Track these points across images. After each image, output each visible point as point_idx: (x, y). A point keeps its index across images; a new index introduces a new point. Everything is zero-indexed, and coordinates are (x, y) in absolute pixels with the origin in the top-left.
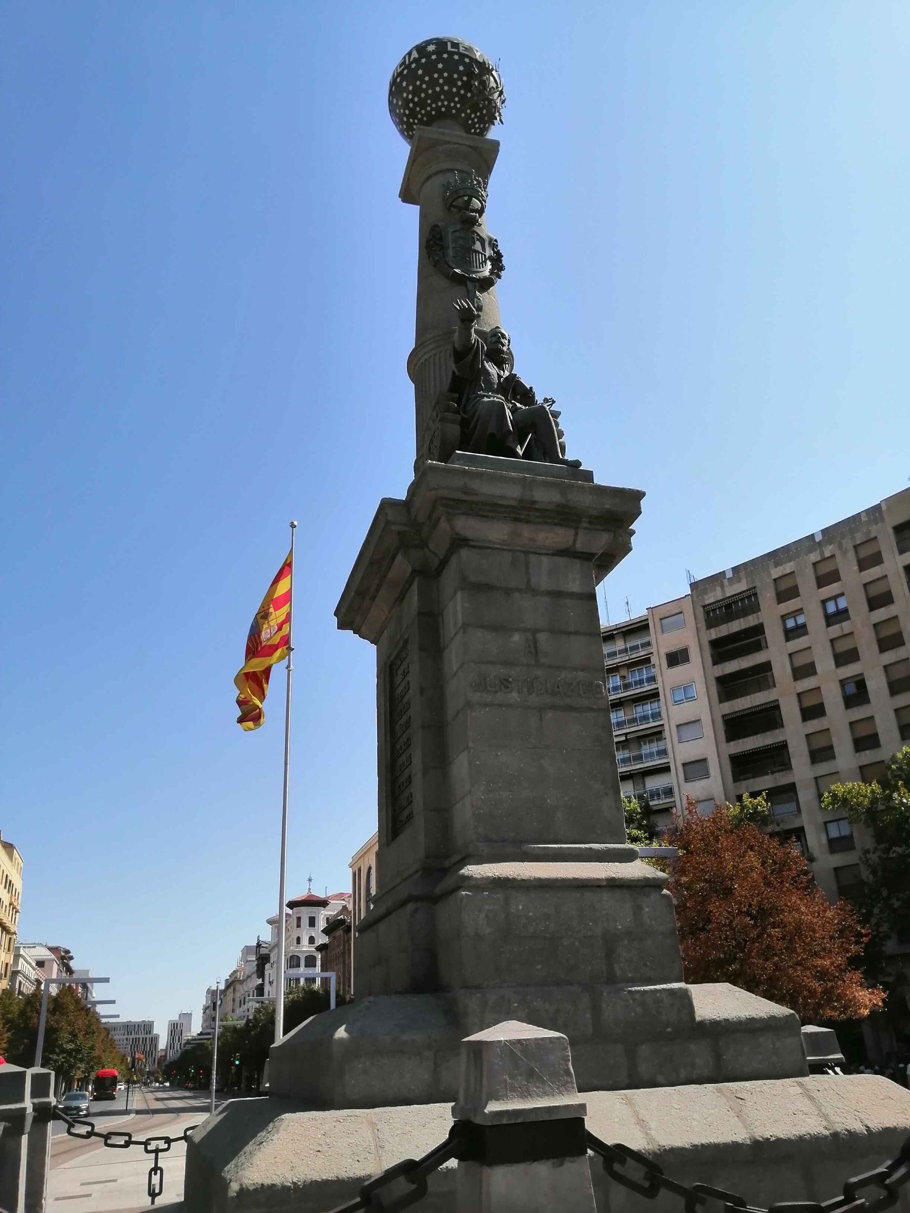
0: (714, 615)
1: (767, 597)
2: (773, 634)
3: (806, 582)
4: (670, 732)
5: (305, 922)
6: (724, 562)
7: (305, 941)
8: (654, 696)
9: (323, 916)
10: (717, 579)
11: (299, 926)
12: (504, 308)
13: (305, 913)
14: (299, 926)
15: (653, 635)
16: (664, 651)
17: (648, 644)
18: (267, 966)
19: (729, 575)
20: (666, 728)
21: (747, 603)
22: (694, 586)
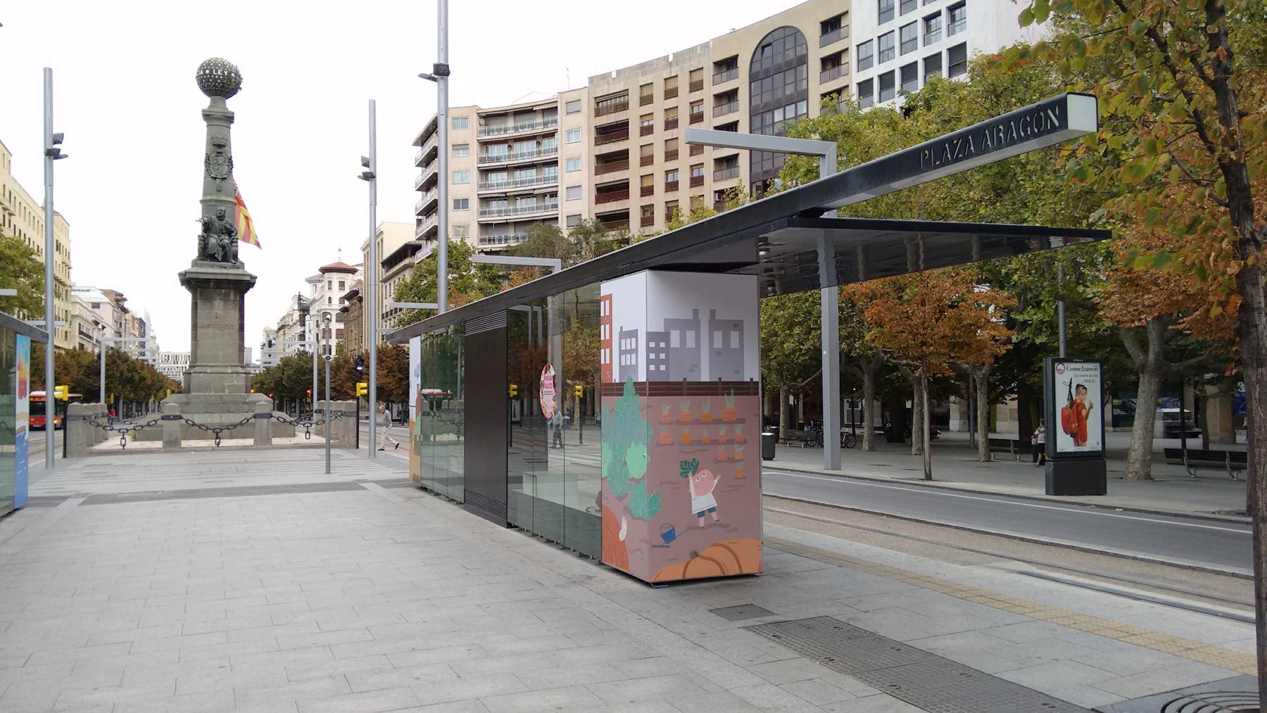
0: (602, 104)
1: (634, 99)
2: (634, 129)
3: (658, 92)
4: (562, 193)
5: (336, 285)
6: (611, 67)
7: (336, 301)
8: (554, 163)
9: (350, 280)
10: (605, 77)
11: (330, 288)
12: (240, 175)
13: (336, 278)
14: (330, 288)
15: (559, 117)
16: (565, 128)
17: (556, 122)
18: (307, 318)
19: (614, 75)
20: (559, 189)
21: (617, 101)
22: (591, 79)
